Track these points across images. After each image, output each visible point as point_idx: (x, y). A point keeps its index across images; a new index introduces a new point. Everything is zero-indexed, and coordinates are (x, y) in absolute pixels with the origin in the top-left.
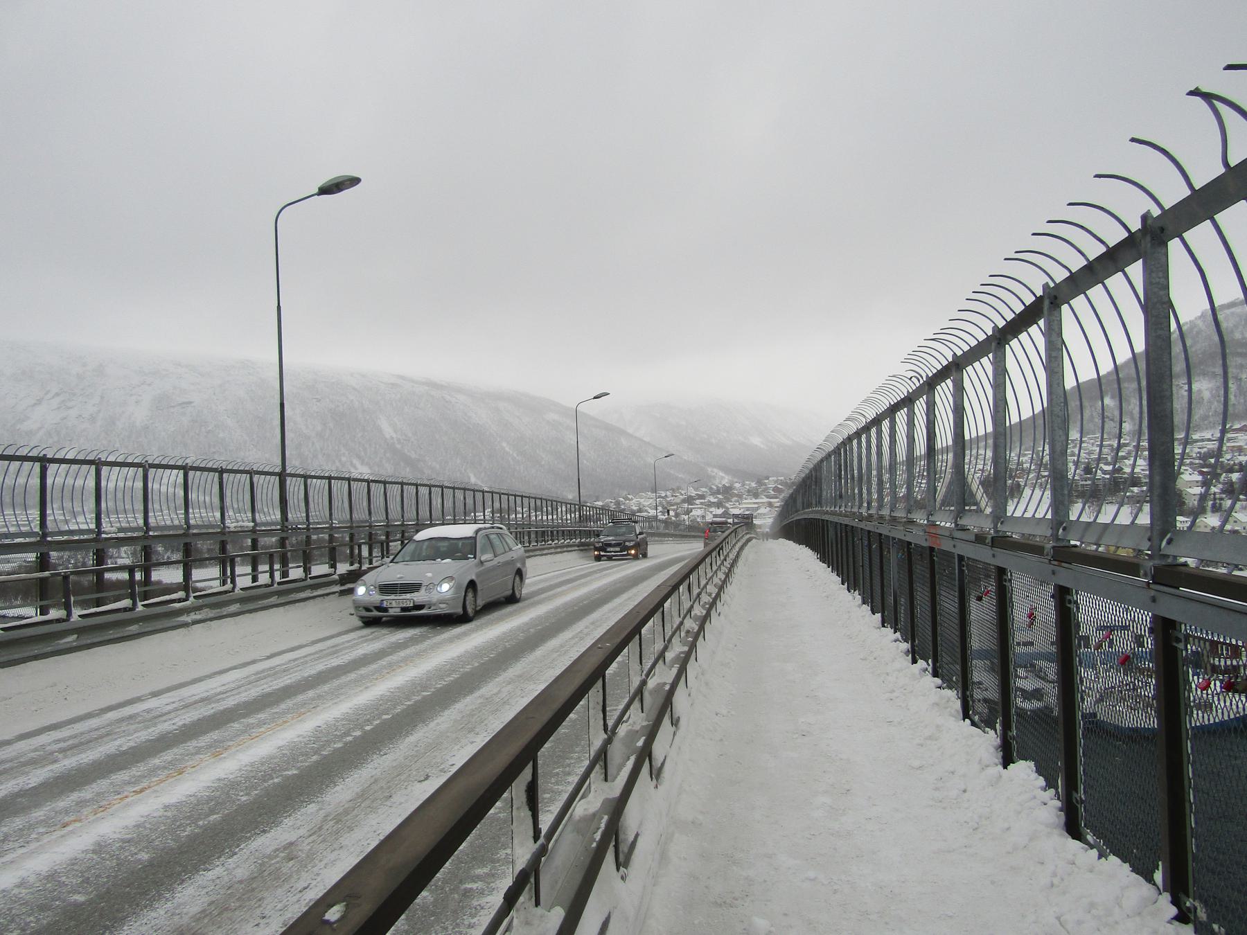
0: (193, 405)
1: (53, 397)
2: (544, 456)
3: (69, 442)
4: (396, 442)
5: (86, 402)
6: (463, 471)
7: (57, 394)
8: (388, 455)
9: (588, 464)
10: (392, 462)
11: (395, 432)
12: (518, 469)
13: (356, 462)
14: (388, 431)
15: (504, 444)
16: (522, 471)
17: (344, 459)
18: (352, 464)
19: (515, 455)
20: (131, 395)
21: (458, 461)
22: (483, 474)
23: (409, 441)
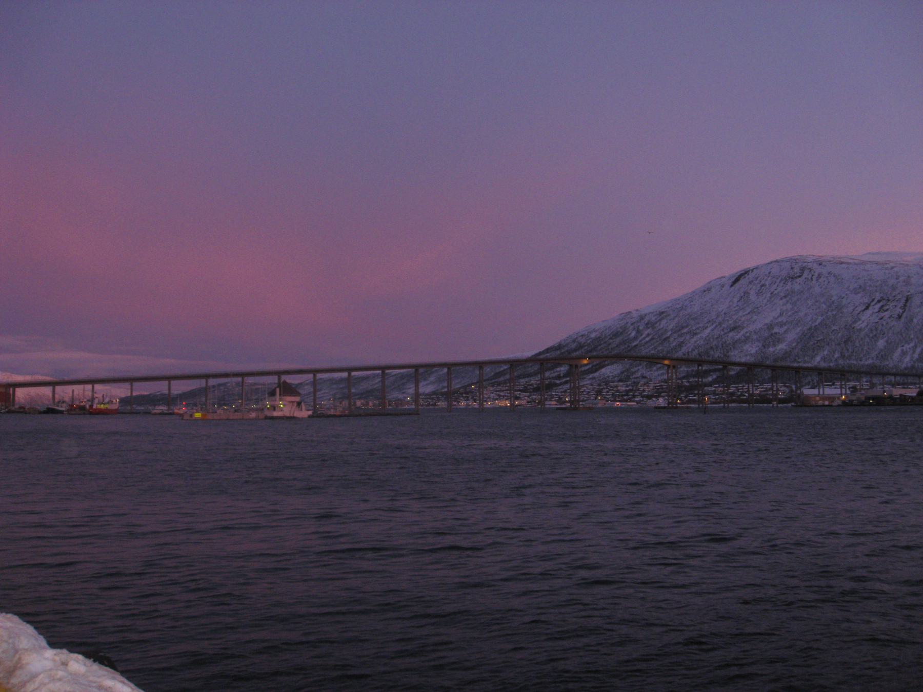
1: (876, 304)
7: (879, 301)
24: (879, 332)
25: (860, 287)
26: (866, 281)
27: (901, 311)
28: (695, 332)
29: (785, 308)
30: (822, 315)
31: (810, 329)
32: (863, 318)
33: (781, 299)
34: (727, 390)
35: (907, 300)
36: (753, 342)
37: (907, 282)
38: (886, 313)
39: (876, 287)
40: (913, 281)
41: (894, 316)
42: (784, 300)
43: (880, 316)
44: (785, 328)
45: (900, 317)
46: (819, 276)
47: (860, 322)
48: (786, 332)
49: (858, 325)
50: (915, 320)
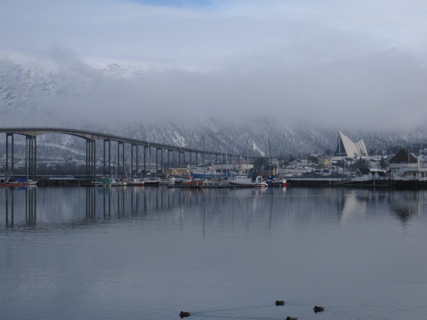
1: (4, 92)
5: (21, 94)
7: (6, 90)
12: (290, 141)
13: (177, 134)
16: (293, 143)
17: (168, 132)
18: (173, 135)
20: (46, 90)
22: (263, 144)
37: (28, 75)
40: (33, 74)
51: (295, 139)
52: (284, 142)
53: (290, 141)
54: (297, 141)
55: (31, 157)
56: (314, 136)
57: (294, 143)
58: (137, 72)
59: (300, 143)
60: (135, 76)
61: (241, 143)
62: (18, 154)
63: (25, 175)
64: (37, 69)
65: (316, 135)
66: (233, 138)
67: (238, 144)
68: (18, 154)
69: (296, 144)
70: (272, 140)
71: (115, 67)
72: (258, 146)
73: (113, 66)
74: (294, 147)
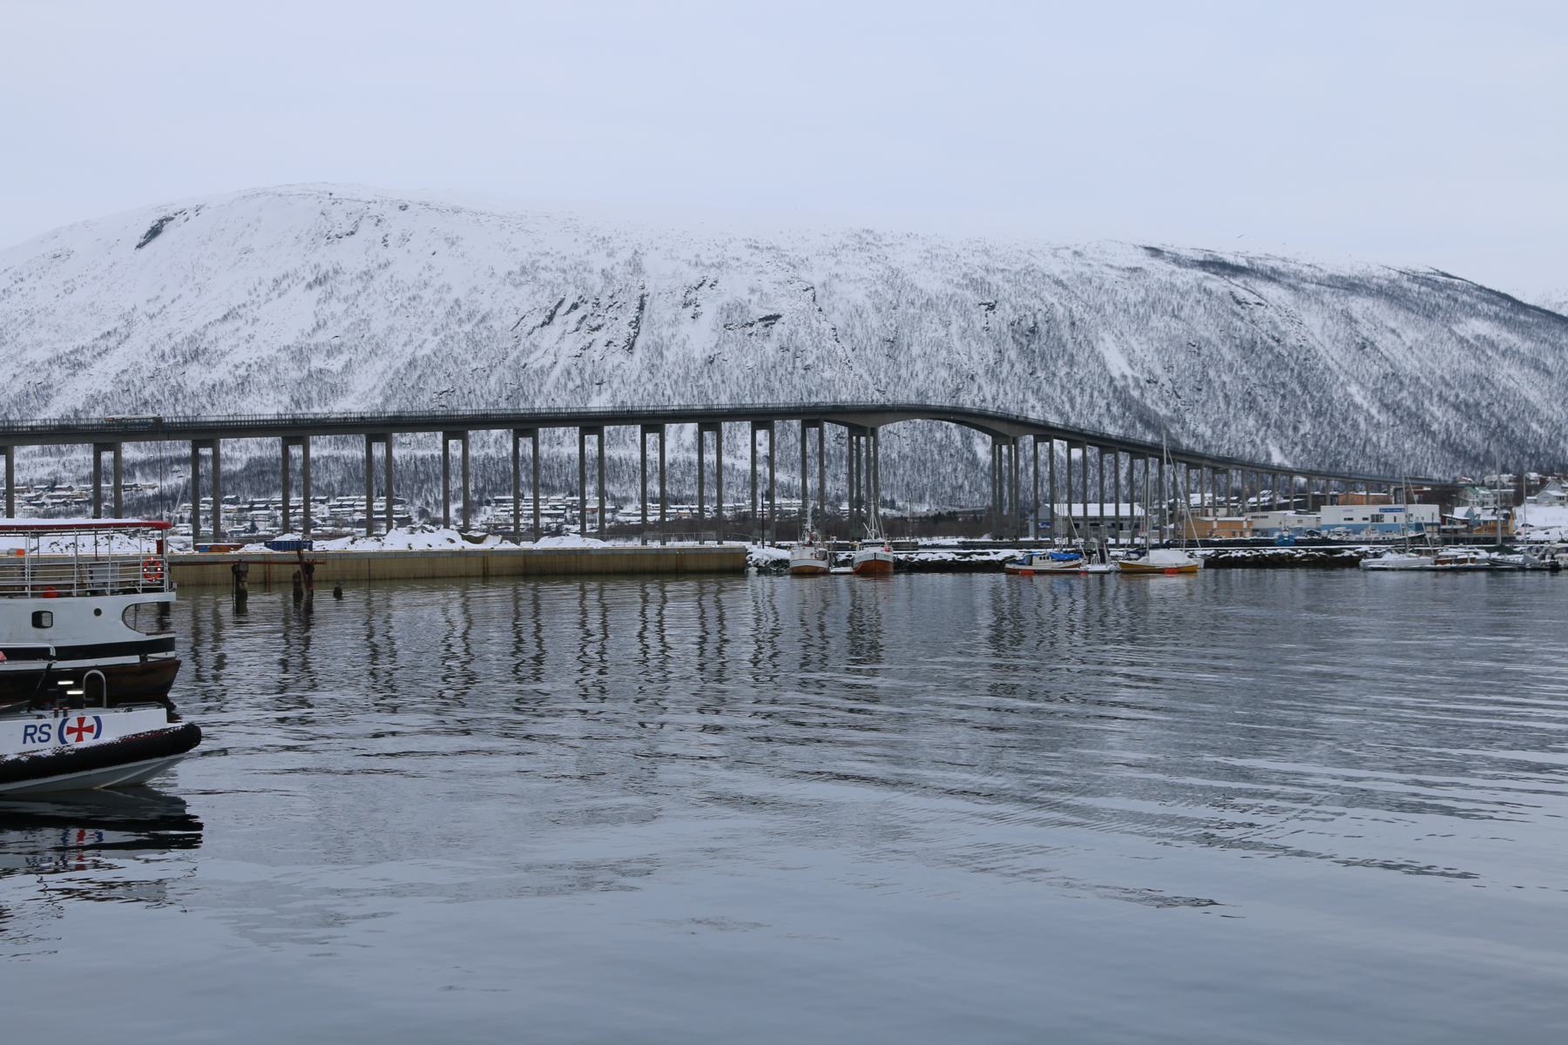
0: (780, 320)
1: (568, 312)
2: (1439, 414)
3: (597, 387)
4: (1132, 385)
6: (1258, 441)
7: (575, 306)
8: (1114, 409)
9: (1541, 431)
10: (1120, 422)
11: (1131, 363)
12: (1375, 439)
14: (1117, 365)
15: (1353, 389)
16: (1383, 444)
19: (1374, 411)
21: (1251, 422)
22: (1298, 449)
23: (1156, 382)
24: (587, 376)
25: (524, 271)
26: (535, 257)
27: (632, 331)
28: (72, 358)
29: (328, 312)
30: (435, 333)
31: (412, 364)
32: (545, 345)
33: (310, 286)
34: (614, 511)
35: (641, 307)
36: (264, 391)
38: (596, 334)
39: (564, 271)
41: (616, 342)
42: (318, 291)
43: (585, 342)
44: (344, 358)
45: (631, 346)
46: (405, 239)
47: (539, 353)
48: (348, 367)
49: (536, 361)
50: (670, 355)
51: (1388, 435)
52: (1358, 441)
53: (1374, 439)
54: (1393, 439)
55: (855, 491)
56: (1440, 424)
57: (1387, 445)
58: (934, 252)
59: (1403, 443)
60: (928, 261)
61: (1236, 446)
62: (621, 485)
63: (1021, 539)
64: (657, 249)
65: (1445, 419)
66: (1214, 432)
67: (1229, 449)
68: (621, 485)
69: (1391, 448)
70: (1323, 438)
71: (870, 239)
72: (1286, 456)
73: (864, 235)
74: (1385, 456)
